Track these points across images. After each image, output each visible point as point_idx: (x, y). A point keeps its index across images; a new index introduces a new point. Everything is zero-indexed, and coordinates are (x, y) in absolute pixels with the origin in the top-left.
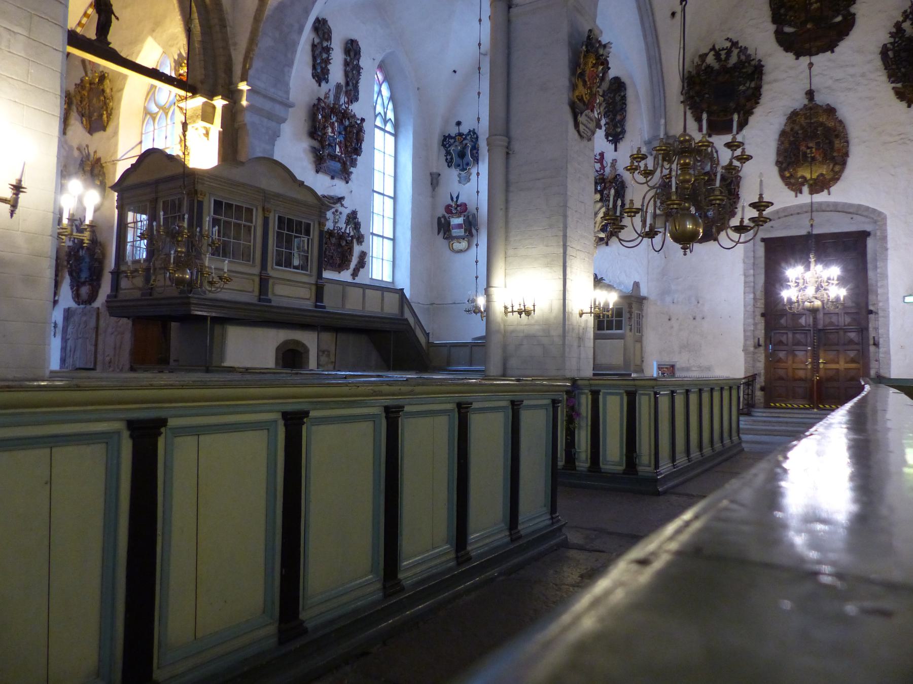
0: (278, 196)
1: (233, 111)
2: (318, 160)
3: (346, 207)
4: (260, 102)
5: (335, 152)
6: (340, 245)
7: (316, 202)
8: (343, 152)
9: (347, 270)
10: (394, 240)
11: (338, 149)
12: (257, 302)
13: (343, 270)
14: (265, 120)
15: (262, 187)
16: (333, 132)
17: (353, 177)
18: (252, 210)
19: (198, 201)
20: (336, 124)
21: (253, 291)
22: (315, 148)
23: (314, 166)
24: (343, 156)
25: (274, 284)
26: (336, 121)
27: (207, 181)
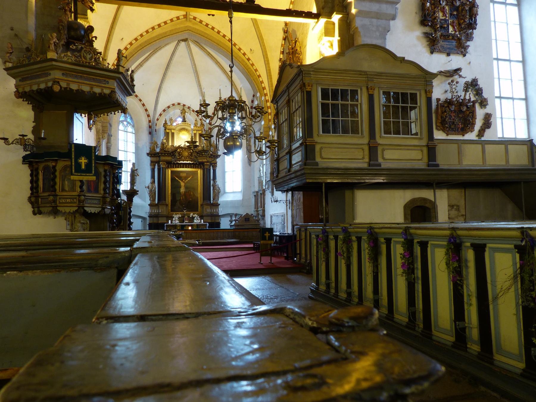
1: (348, 22)
2: (431, 42)
3: (465, 77)
6: (461, 111)
7: (420, 73)
8: (457, 30)
9: (472, 132)
10: (526, 99)
11: (451, 29)
13: (467, 133)
14: (374, 21)
15: (364, 69)
16: (444, 15)
17: (470, 50)
18: (357, 91)
19: (307, 91)
20: (447, 8)
22: (427, 33)
23: (428, 49)
24: (457, 33)
25: (383, 150)
26: (446, 5)
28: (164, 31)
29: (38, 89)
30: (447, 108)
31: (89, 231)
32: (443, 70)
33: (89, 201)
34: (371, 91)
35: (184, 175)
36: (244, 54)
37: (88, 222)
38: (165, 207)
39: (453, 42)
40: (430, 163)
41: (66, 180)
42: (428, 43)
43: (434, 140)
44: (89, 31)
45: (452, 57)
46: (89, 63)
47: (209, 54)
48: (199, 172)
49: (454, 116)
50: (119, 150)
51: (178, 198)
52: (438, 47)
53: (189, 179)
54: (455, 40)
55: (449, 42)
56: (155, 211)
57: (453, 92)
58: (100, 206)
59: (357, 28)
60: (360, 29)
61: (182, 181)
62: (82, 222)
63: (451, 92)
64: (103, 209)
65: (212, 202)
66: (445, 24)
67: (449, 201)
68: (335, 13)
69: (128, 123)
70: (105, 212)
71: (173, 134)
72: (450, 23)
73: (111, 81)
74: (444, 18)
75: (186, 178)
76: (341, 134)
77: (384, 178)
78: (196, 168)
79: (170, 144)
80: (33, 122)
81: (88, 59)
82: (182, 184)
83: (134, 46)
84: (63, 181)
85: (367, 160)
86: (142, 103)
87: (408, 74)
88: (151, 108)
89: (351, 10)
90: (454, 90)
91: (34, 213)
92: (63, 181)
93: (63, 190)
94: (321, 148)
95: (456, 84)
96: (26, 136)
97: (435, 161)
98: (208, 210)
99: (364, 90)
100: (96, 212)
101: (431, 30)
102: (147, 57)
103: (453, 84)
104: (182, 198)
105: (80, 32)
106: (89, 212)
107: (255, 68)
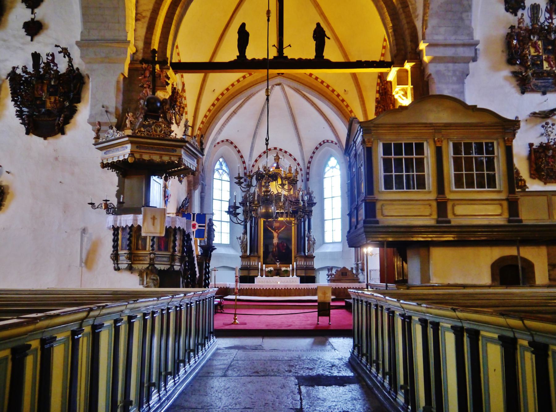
0: (447, 126)
4: (441, 52)
5: (543, 68)
8: (553, 66)
11: (545, 65)
12: (506, 223)
14: (451, 65)
16: (537, 50)
18: (423, 144)
20: (540, 43)
21: (430, 215)
23: (519, 89)
25: (453, 206)
26: (539, 39)
27: (374, 130)
28: (255, 78)
29: (117, 161)
30: (542, 154)
31: (160, 287)
32: (537, 111)
33: (160, 259)
34: (438, 143)
36: (338, 95)
37: (158, 278)
38: (256, 259)
39: (549, 79)
40: (511, 218)
41: (140, 239)
42: (517, 83)
43: (517, 193)
44: (164, 104)
45: (549, 96)
46: (159, 135)
47: (304, 96)
49: (553, 162)
50: (213, 199)
51: (271, 250)
52: (531, 86)
53: (283, 229)
54: (551, 76)
55: (544, 79)
56: (246, 263)
57: (549, 135)
58: (169, 263)
59: (430, 75)
60: (433, 76)
61: (275, 231)
62: (152, 277)
63: (546, 135)
64: (172, 266)
65: (306, 254)
66: (537, 61)
67: (549, 259)
68: (406, 61)
69: (224, 170)
70: (174, 268)
72: (544, 58)
73: (178, 149)
74: (536, 54)
75: (279, 228)
76: (405, 190)
77: (455, 236)
80: (117, 186)
81: (158, 132)
82: (275, 235)
83: (225, 97)
85: (435, 216)
86: (238, 150)
87: (481, 123)
88: (246, 154)
89: (423, 57)
90: (550, 133)
91: (115, 270)
92: (138, 240)
94: (383, 205)
95: (552, 126)
96: (109, 201)
97: (518, 216)
98: (302, 263)
99: (431, 142)
100: (166, 269)
101: (520, 69)
102: (241, 104)
103: (549, 126)
104: (274, 250)
105: (157, 106)
106: (159, 269)
107: (350, 110)
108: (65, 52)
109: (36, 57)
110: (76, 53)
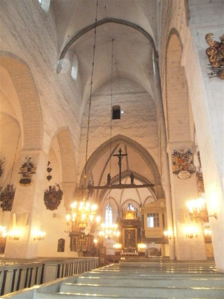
35: (130, 231)
36: (150, 182)
48: (136, 229)
51: (127, 241)
71: (125, 214)
78: (135, 228)
79: (124, 218)
82: (129, 235)
84: (77, 242)
93: (77, 244)
108: (58, 185)
109: (50, 187)
110: (61, 186)
